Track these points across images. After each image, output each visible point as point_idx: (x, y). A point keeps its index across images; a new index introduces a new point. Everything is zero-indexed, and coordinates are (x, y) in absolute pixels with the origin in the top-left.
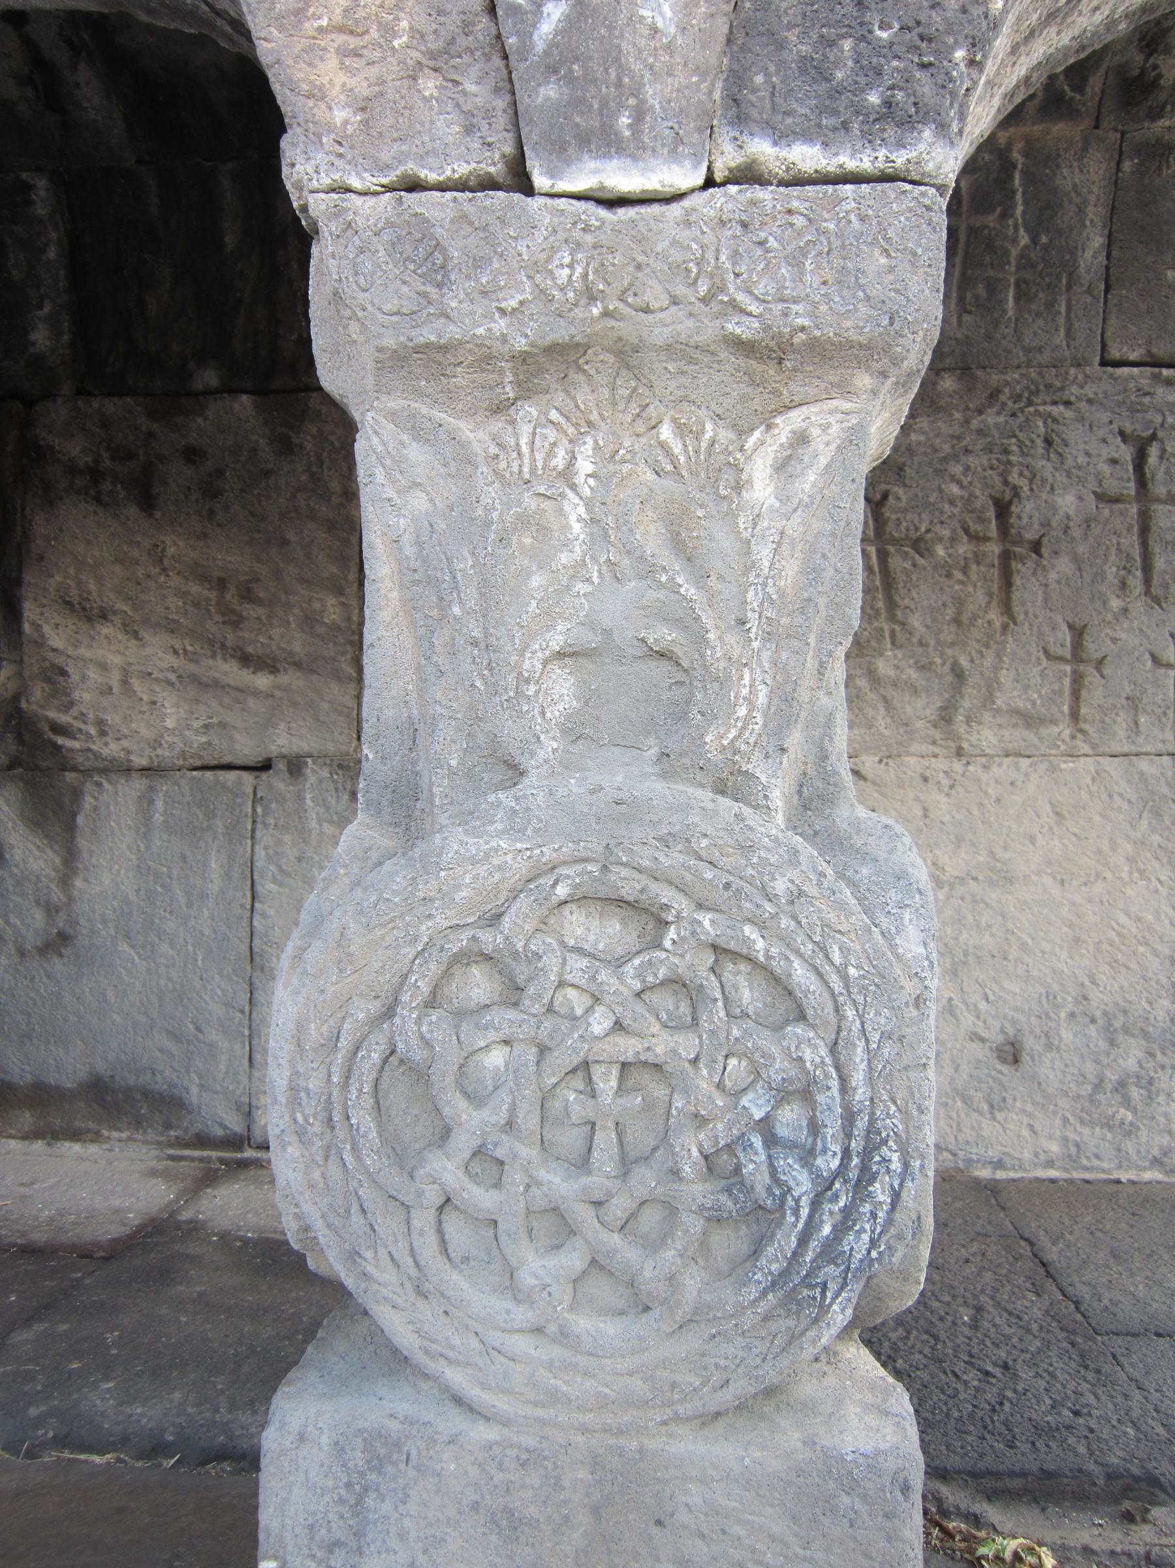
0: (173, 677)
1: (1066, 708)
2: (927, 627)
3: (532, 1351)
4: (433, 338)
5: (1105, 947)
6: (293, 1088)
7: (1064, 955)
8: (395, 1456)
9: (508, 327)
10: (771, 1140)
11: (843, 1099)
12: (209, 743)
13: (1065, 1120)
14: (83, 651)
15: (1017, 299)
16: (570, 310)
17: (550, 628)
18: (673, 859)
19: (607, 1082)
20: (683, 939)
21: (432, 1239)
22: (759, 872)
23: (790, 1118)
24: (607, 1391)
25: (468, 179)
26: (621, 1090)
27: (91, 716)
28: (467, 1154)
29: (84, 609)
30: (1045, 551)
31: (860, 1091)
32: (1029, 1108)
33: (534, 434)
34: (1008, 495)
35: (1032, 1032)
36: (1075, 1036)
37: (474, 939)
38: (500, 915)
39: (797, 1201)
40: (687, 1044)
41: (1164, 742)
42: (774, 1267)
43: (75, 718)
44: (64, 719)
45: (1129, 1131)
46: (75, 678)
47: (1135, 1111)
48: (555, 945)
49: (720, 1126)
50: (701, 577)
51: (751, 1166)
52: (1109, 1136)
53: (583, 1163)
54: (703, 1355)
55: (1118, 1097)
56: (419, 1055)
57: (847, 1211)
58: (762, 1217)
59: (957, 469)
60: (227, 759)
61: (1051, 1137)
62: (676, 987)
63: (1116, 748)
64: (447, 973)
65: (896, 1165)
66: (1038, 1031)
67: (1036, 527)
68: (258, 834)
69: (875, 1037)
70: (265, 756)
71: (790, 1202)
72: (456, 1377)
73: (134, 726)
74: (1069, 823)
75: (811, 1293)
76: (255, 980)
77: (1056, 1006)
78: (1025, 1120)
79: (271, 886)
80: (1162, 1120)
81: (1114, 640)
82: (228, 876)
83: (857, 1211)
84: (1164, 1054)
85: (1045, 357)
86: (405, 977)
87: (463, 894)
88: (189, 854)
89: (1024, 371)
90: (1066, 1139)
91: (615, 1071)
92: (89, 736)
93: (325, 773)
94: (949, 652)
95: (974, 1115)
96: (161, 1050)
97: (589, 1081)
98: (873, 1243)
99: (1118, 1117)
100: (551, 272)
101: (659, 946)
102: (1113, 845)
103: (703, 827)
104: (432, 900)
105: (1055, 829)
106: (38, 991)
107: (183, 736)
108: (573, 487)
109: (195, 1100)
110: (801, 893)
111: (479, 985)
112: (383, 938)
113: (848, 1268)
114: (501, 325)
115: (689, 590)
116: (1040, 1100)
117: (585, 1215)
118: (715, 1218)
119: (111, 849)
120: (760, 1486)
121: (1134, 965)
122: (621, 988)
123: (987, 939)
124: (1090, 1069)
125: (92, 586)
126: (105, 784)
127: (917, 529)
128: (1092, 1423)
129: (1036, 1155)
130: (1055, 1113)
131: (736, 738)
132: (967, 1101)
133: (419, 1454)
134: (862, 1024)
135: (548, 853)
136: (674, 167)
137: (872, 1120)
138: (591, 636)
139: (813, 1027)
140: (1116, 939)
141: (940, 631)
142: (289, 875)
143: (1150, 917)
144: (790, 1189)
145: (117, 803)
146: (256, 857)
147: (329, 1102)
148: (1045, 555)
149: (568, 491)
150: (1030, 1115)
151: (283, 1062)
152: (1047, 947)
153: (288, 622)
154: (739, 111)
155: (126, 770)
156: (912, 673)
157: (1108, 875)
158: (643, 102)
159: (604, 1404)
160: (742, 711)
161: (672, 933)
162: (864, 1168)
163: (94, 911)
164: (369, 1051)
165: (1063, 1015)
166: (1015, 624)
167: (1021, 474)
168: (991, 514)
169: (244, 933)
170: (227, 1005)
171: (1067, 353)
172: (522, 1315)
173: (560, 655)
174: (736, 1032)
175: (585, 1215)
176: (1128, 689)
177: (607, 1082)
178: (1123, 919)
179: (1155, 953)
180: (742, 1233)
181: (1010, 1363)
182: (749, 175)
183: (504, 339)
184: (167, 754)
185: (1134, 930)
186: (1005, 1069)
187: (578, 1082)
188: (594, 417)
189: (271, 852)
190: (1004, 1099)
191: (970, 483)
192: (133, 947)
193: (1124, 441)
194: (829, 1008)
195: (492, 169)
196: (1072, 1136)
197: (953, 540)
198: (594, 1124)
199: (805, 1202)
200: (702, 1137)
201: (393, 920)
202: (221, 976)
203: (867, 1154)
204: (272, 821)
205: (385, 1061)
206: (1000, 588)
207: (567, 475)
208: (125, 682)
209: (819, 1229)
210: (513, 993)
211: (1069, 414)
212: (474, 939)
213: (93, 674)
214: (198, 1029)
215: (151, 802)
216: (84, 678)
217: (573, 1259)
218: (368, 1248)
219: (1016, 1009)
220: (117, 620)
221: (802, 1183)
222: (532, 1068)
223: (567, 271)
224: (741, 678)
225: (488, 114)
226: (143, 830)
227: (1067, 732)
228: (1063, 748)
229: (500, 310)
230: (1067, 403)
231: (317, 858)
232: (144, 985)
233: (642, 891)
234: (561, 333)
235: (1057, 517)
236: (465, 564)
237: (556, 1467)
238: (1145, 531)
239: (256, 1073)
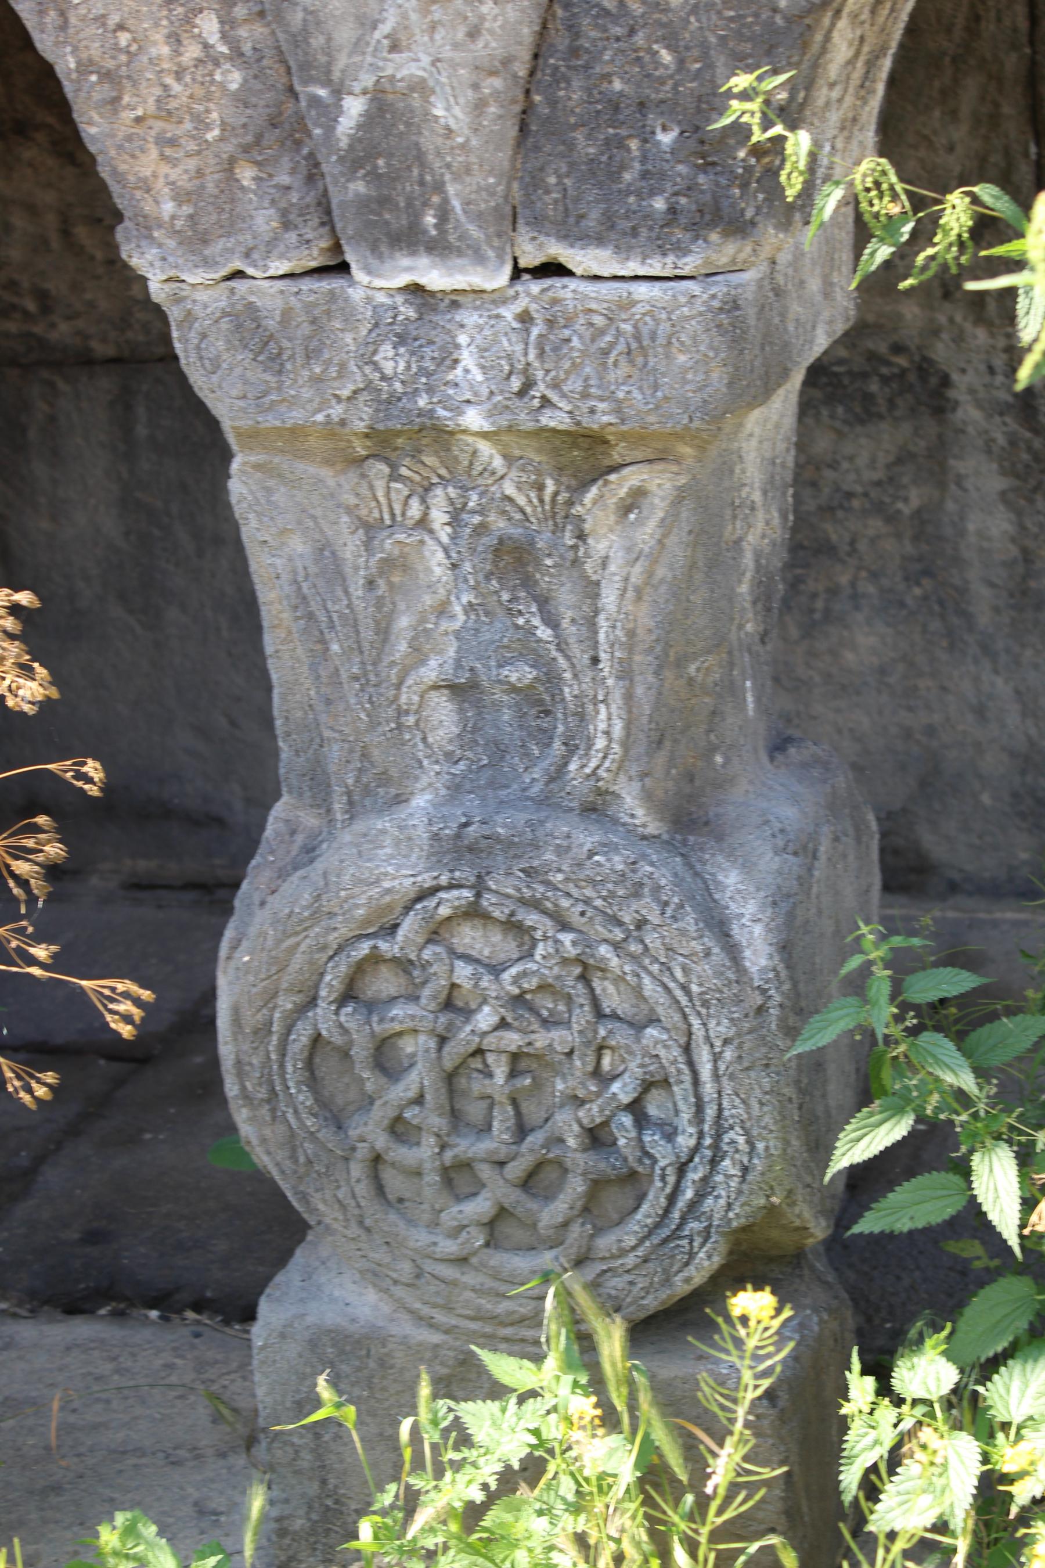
4: (278, 423)
6: (239, 1063)
10: (641, 1120)
17: (423, 662)
27: (26, 285)
37: (375, 947)
38: (396, 926)
56: (338, 1040)
57: (705, 1179)
69: (718, 1043)
71: (658, 1172)
73: (88, 296)
92: (26, 313)
108: (431, 532)
114: (337, 411)
131: (598, 767)
136: (479, 269)
149: (427, 538)
155: (86, 361)
158: (446, 201)
160: (600, 743)
162: (716, 1146)
173: (436, 687)
174: (602, 1032)
184: (141, 338)
188: (443, 472)
203: (718, 1137)
207: (423, 523)
208: (66, 233)
209: (683, 1192)
212: (375, 947)
213: (19, 220)
214: (233, 723)
220: (41, 137)
221: (664, 1155)
223: (391, 364)
224: (597, 712)
229: (336, 396)
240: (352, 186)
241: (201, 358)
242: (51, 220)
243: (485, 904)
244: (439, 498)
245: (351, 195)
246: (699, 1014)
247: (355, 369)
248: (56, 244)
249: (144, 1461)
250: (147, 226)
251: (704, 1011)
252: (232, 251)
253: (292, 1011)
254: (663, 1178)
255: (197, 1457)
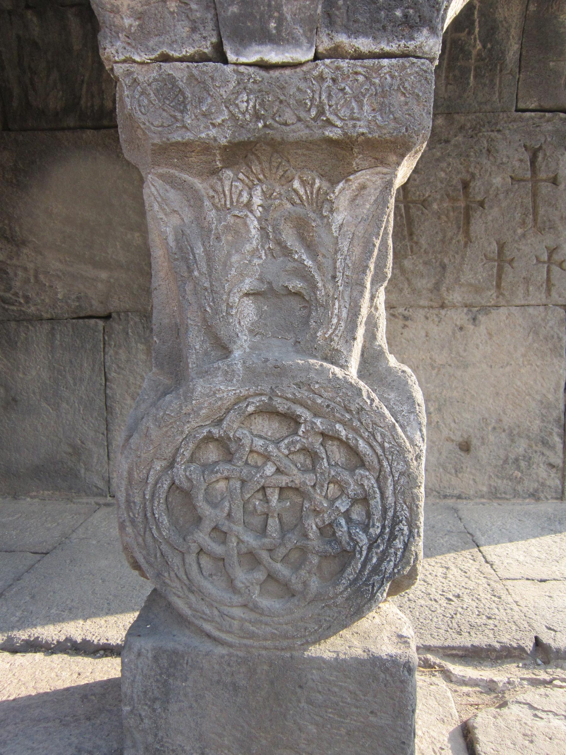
0: (60, 274)
1: (494, 283)
2: (429, 244)
3: (242, 615)
4: (180, 139)
5: (510, 396)
6: (128, 501)
7: (491, 401)
8: (181, 661)
9: (217, 133)
10: (349, 520)
11: (382, 502)
12: (80, 306)
13: (490, 477)
14: (15, 261)
15: (475, 77)
16: (248, 124)
17: (242, 281)
18: (303, 394)
19: (274, 498)
20: (308, 431)
21: (195, 567)
22: (343, 400)
23: (357, 514)
24: (276, 631)
25: (194, 56)
26: (280, 499)
27: (21, 294)
28: (209, 530)
29: (14, 240)
30: (486, 206)
31: (390, 499)
32: (473, 471)
33: (231, 185)
34: (468, 178)
35: (475, 436)
36: (495, 438)
37: (210, 432)
39: (361, 548)
40: (310, 479)
41: (541, 299)
42: (351, 577)
43: (13, 295)
44: (8, 295)
45: (520, 481)
46: (11, 274)
47: (522, 472)
48: (248, 434)
49: (326, 515)
50: (314, 255)
51: (340, 533)
52: (510, 483)
53: (263, 531)
54: (319, 615)
55: (515, 466)
56: (186, 485)
57: (383, 552)
58: (345, 556)
59: (444, 165)
60: (90, 313)
61: (483, 484)
62: (304, 452)
63: (518, 302)
64: (198, 447)
65: (406, 532)
66: (478, 436)
67: (482, 193)
68: (107, 350)
69: (397, 475)
70: (108, 311)
71: (358, 548)
72: (208, 627)
74: (494, 338)
75: (367, 588)
76: (108, 419)
77: (487, 425)
78: (472, 477)
79: (113, 374)
80: (535, 476)
81: (519, 250)
82: (93, 369)
83: (388, 552)
84: (536, 446)
85: (488, 107)
86: (178, 450)
87: (204, 411)
88: (73, 360)
89: (478, 114)
90: (490, 485)
91: (277, 491)
92: (20, 303)
93: (137, 319)
94: (439, 256)
95: (448, 475)
96: (65, 453)
97: (265, 495)
98: (396, 566)
99: (514, 475)
100: (237, 106)
101: (296, 434)
102: (515, 348)
103: (316, 378)
104: (189, 414)
105: (488, 341)
106: (5, 427)
107: (67, 302)
108: (251, 212)
109: (83, 475)
110: (362, 409)
111: (212, 453)
112: (167, 432)
113: (384, 577)
114: (213, 132)
115: (309, 263)
116: (478, 467)
117: (264, 555)
118: (324, 556)
119: (35, 358)
120: (345, 671)
121: (523, 405)
122: (280, 454)
123: (455, 394)
124: (502, 453)
125: (17, 229)
126: (30, 327)
127: (424, 196)
128: (496, 622)
129: (476, 493)
130: (485, 473)
131: (332, 334)
132: (445, 469)
133: (192, 660)
134: (391, 468)
135: (244, 393)
136: (298, 49)
137: (395, 512)
138: (262, 285)
139: (368, 470)
140: (516, 393)
141: (435, 246)
142: (123, 369)
143: (532, 383)
144: (358, 543)
145: (36, 336)
146: (106, 361)
147: (145, 507)
148: (486, 208)
149: (249, 214)
150: (474, 475)
151: (123, 489)
152: (484, 397)
153: (116, 245)
154: (330, 21)
155: (40, 319)
156: (421, 267)
157: (513, 363)
158: (282, 15)
159: (273, 637)
160: (335, 321)
161: (302, 428)
162: (392, 533)
163: (29, 388)
164: (162, 484)
165: (490, 429)
166: (471, 242)
167: (475, 167)
168: (460, 187)
169: (102, 397)
170: (96, 431)
171: (499, 105)
172: (236, 599)
173: (247, 295)
174: (333, 473)
175: (264, 555)
176: (524, 274)
177: (274, 498)
178: (519, 383)
179: (534, 399)
180: (336, 561)
181: (461, 594)
182: (336, 53)
183: (215, 139)
185: (524, 389)
186: (462, 454)
187: (260, 495)
188: (261, 177)
189: (113, 358)
190: (462, 468)
191: (450, 172)
192: (49, 405)
193: (526, 150)
194: (376, 461)
195: (206, 51)
196: (493, 484)
197: (442, 200)
198: (268, 515)
199: (365, 548)
200: (317, 520)
201: (171, 424)
202: (92, 417)
203: (392, 528)
204: (113, 343)
205: (170, 488)
206: (464, 224)
207: (248, 205)
208: (36, 277)
210: (229, 456)
211: (499, 136)
212: (210, 432)
213: (20, 273)
214: (82, 442)
215: (53, 335)
216: (16, 275)
217: (260, 575)
218: (166, 572)
219: (469, 426)
221: (363, 540)
222: (239, 491)
223: (245, 104)
224: (334, 305)
225: (203, 21)
226: (50, 349)
227: (495, 294)
228: (493, 302)
230: (499, 131)
231: (135, 360)
232: (55, 422)
233: (288, 409)
234: (244, 137)
235: (493, 189)
236: (200, 251)
237: (253, 664)
238: (535, 195)
239: (111, 463)
240: (230, 9)
241: (140, 106)
242: (32, 272)
243: (274, 403)
244: (258, 192)
245: (229, 13)
246: (387, 459)
247: (224, 108)
248: (32, 280)
249: (49, 724)
250: (117, 31)
251: (390, 457)
252: (163, 43)
253: (160, 471)
254: (361, 553)
255: (76, 720)
